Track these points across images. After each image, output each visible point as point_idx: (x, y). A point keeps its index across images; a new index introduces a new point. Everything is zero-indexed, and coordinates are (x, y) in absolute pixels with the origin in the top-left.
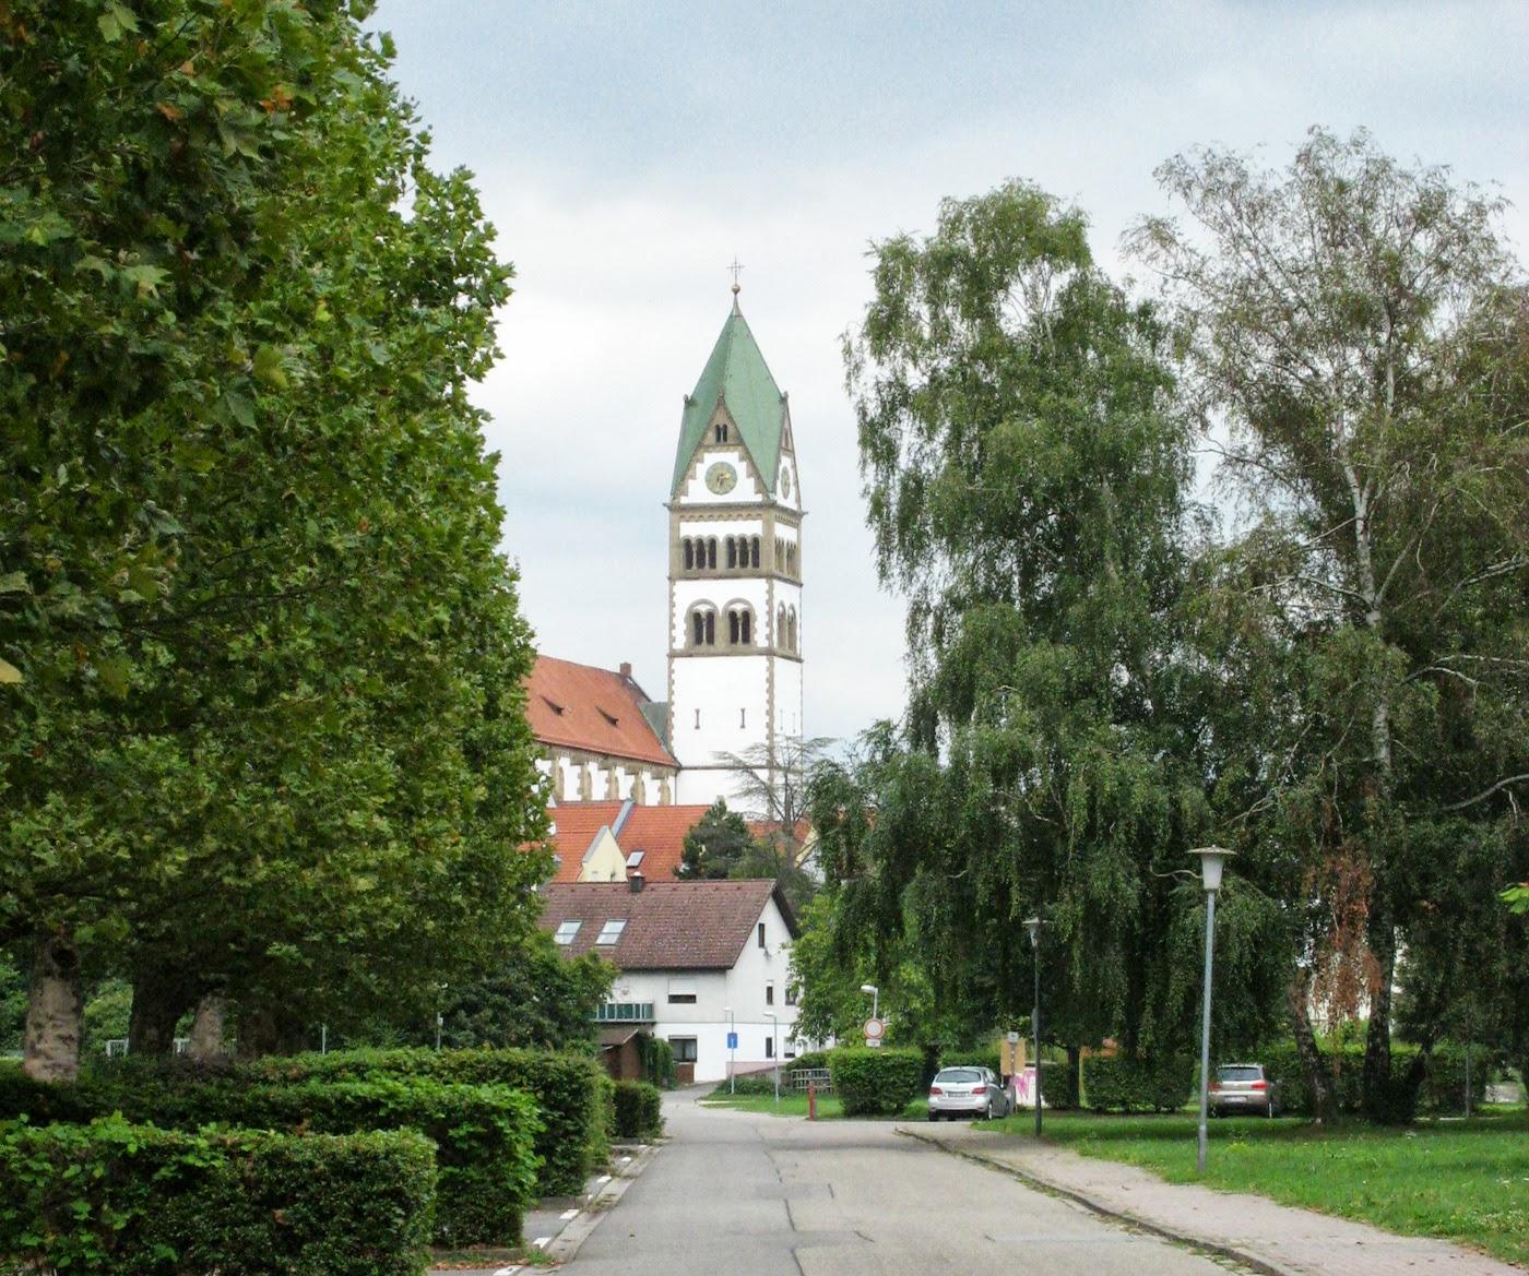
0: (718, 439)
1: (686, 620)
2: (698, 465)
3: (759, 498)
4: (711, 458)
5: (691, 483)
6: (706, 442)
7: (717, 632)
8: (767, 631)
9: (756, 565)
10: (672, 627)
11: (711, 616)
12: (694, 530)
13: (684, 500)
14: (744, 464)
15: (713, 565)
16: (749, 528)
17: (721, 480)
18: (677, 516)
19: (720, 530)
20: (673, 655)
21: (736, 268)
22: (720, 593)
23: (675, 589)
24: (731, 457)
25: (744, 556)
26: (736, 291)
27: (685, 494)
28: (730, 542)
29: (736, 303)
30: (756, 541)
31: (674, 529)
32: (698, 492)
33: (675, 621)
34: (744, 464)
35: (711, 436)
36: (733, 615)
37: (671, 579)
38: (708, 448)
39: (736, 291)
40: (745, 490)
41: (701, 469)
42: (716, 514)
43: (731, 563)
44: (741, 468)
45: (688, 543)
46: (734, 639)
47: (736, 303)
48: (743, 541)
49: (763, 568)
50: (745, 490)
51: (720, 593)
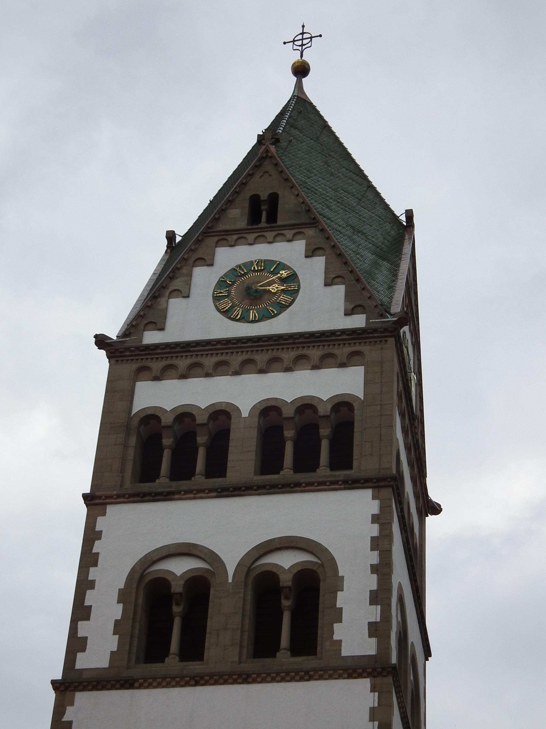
1: (123, 597)
5: (176, 307)
7: (214, 622)
8: (374, 613)
10: (81, 611)
11: (199, 589)
14: (319, 263)
15: (217, 465)
18: (128, 368)
20: (68, 686)
21: (303, 40)
22: (229, 528)
23: (101, 524)
24: (290, 252)
25: (307, 449)
28: (269, 411)
29: (299, 86)
30: (343, 405)
31: (117, 394)
32: (194, 318)
33: (90, 598)
34: (319, 263)
36: (263, 585)
37: (95, 501)
40: (320, 306)
44: (312, 271)
45: (151, 418)
46: (263, 644)
47: (299, 86)
49: (364, 463)
50: (320, 306)
51: (229, 528)
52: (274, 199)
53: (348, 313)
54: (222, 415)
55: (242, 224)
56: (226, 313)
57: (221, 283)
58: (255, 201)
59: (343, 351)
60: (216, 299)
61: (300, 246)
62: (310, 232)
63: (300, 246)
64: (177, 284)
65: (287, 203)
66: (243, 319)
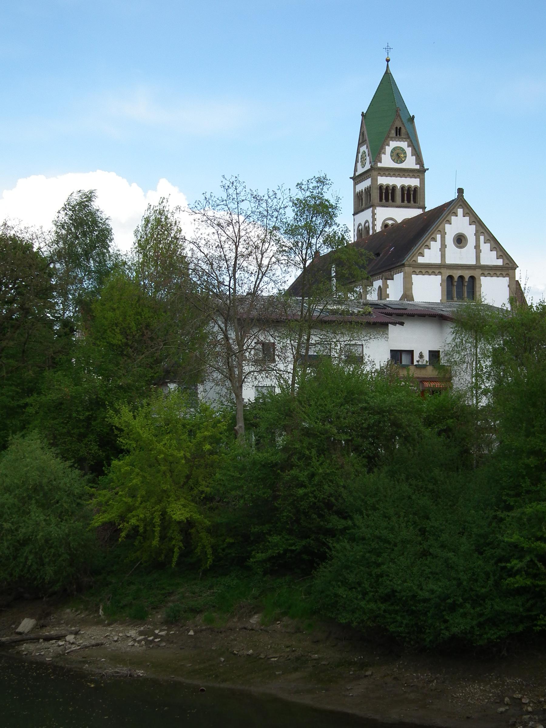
0: (396, 135)
2: (387, 147)
3: (418, 167)
4: (393, 144)
6: (391, 136)
9: (415, 202)
12: (383, 181)
13: (379, 165)
14: (410, 148)
15: (393, 200)
16: (414, 182)
17: (398, 155)
19: (399, 182)
24: (404, 145)
26: (388, 61)
27: (381, 162)
28: (403, 188)
30: (416, 188)
34: (410, 148)
35: (393, 132)
38: (392, 139)
39: (388, 61)
41: (388, 149)
42: (397, 174)
43: (403, 201)
44: (409, 151)
45: (381, 187)
48: (409, 187)
52: (400, 128)
53: (416, 164)
54: (394, 187)
55: (395, 135)
56: (393, 160)
57: (392, 152)
58: (396, 128)
59: (416, 175)
60: (391, 156)
61: (406, 143)
62: (408, 140)
63: (406, 143)
64: (383, 151)
65: (403, 130)
66: (397, 163)
